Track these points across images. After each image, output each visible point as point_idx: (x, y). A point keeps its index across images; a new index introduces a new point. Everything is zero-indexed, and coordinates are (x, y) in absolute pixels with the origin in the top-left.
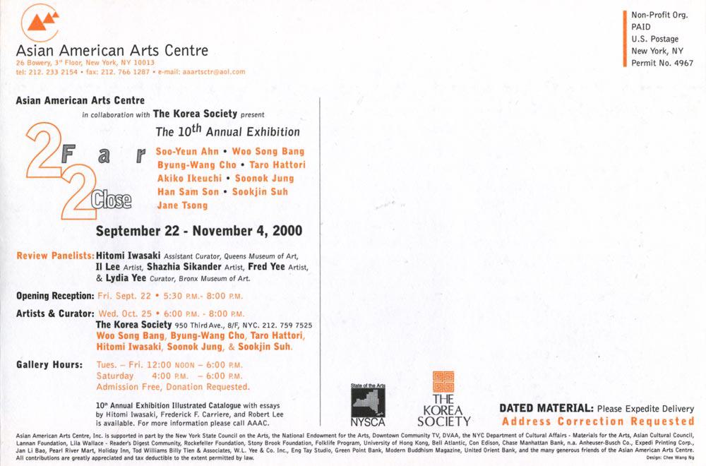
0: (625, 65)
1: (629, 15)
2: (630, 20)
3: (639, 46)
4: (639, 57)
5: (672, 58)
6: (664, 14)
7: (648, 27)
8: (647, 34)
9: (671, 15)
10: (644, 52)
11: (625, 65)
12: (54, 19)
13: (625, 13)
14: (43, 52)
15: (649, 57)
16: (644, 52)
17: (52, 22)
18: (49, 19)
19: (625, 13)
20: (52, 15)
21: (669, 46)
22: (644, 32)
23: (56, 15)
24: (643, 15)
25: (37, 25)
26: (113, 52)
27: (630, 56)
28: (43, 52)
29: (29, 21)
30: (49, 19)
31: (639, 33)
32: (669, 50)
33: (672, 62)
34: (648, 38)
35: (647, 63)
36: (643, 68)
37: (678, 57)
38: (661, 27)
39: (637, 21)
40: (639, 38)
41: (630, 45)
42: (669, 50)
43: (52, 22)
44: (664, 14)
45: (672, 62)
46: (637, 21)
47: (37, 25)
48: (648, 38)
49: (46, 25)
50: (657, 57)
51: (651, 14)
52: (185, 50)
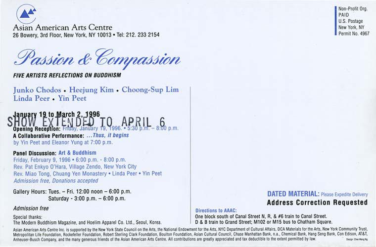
0: (336, 34)
1: (338, 9)
2: (338, 12)
3: (343, 25)
4: (343, 31)
5: (359, 31)
6: (355, 9)
7: (347, 15)
8: (347, 19)
9: (359, 9)
10: (345, 28)
11: (336, 34)
12: (34, 12)
13: (336, 7)
14: (27, 29)
15: (347, 30)
16: (345, 28)
17: (33, 14)
18: (31, 12)
19: (336, 7)
20: (32, 10)
21: (357, 25)
22: (345, 18)
23: (35, 10)
24: (345, 9)
25: (25, 15)
26: (64, 28)
27: (338, 30)
28: (27, 29)
29: (20, 13)
30: (31, 12)
31: (342, 18)
32: (357, 27)
33: (359, 33)
34: (347, 21)
35: (346, 33)
36: (344, 36)
37: (362, 30)
38: (353, 15)
39: (341, 12)
40: (342, 21)
41: (338, 24)
42: (357, 27)
43: (33, 14)
44: (355, 9)
45: (359, 33)
46: (341, 12)
47: (25, 15)
48: (347, 21)
49: (29, 15)
50: (351, 31)
51: (349, 8)
52: (101, 28)
